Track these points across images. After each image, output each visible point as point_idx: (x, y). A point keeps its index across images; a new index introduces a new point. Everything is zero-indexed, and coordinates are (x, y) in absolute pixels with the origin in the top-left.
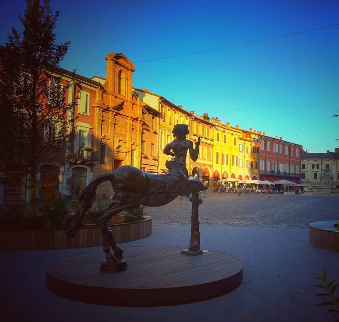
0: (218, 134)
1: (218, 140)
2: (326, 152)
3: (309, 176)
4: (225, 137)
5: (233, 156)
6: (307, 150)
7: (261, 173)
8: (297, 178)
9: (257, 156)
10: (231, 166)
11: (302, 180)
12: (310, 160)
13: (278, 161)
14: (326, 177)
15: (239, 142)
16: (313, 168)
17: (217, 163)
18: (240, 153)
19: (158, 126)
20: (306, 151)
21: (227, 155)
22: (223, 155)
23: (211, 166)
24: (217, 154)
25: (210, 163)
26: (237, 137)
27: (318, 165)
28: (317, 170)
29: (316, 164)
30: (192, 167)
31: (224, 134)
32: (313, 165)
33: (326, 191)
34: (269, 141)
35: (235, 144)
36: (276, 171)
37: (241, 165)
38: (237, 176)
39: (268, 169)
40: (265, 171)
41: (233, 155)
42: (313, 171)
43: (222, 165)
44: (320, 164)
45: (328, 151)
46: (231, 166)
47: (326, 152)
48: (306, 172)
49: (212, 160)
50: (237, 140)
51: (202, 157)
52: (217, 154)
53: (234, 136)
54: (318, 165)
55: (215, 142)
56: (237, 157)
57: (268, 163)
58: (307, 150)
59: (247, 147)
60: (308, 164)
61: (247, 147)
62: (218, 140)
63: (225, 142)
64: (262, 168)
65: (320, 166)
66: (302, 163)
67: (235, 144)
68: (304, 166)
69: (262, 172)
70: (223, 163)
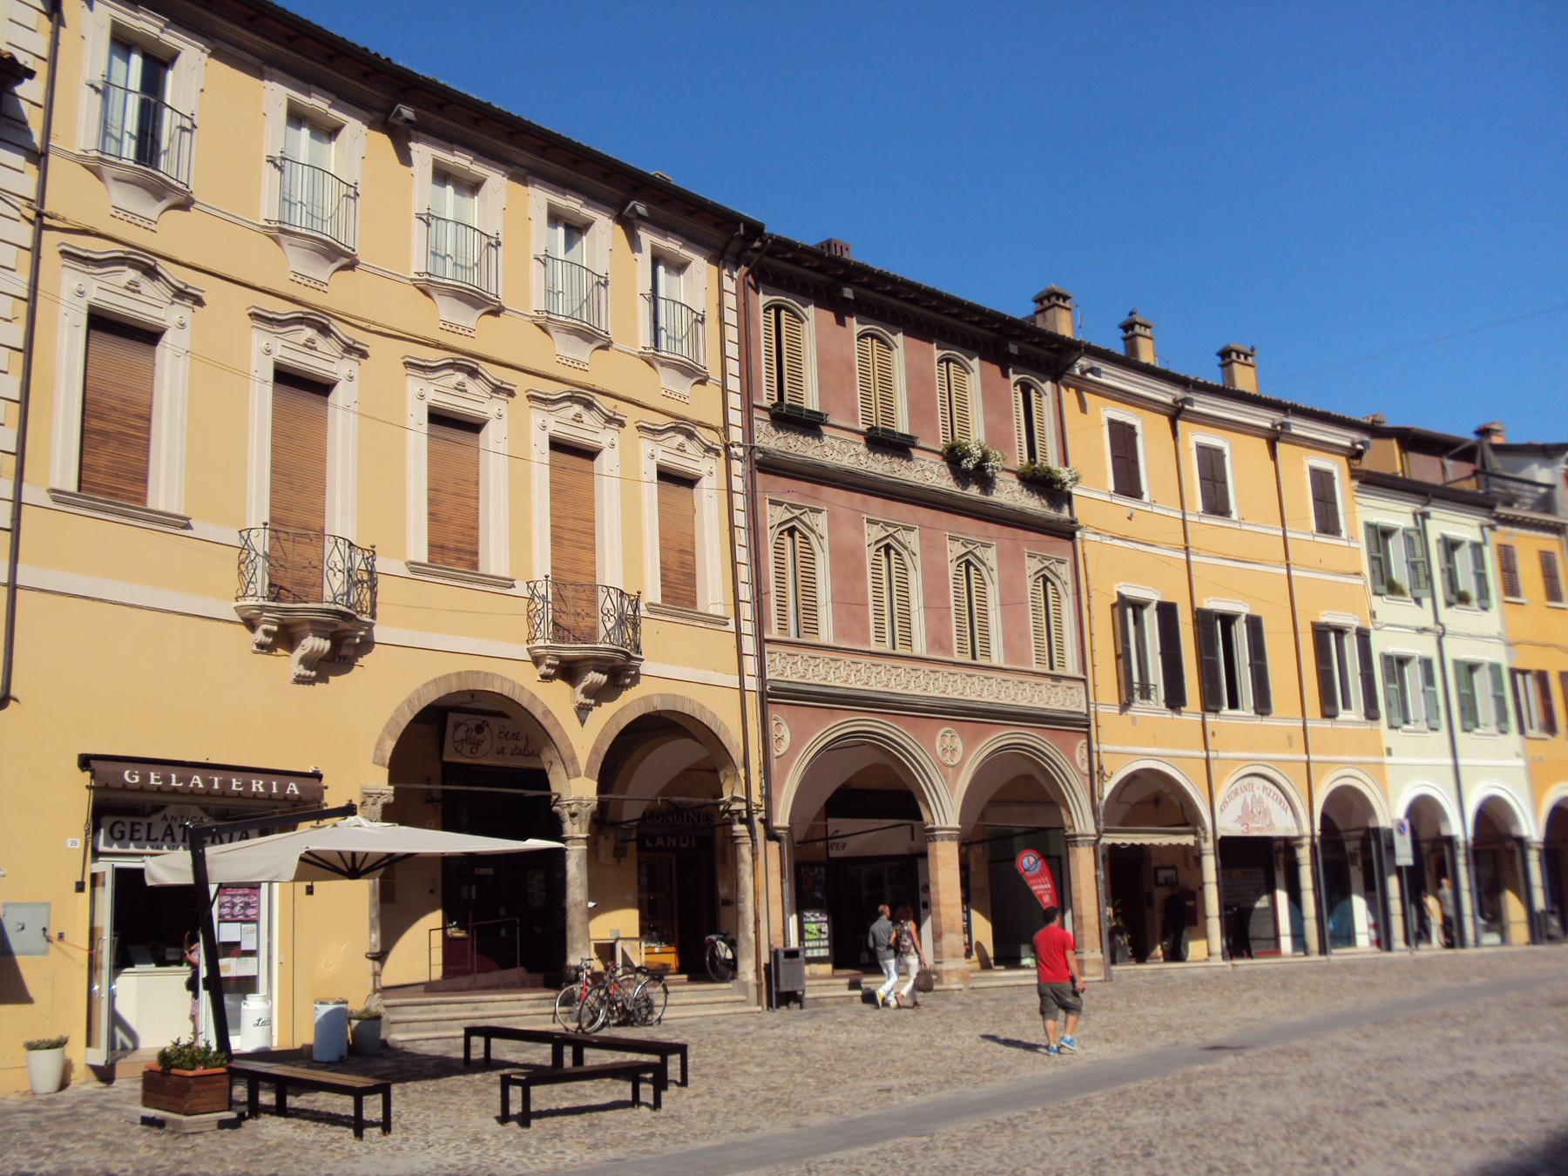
0: (1123, 437)
1: (1128, 483)
4: (1211, 462)
5: (1321, 633)
18: (1390, 610)
21: (1254, 624)
23: (1079, 725)
26: (1337, 467)
30: (794, 748)
31: (1194, 436)
35: (1328, 522)
41: (1326, 617)
43: (1210, 718)
46: (1316, 723)
49: (1072, 668)
50: (1343, 486)
51: (937, 641)
53: (1300, 464)
56: (1363, 636)
62: (1128, 483)
63: (1217, 504)
67: (1328, 522)
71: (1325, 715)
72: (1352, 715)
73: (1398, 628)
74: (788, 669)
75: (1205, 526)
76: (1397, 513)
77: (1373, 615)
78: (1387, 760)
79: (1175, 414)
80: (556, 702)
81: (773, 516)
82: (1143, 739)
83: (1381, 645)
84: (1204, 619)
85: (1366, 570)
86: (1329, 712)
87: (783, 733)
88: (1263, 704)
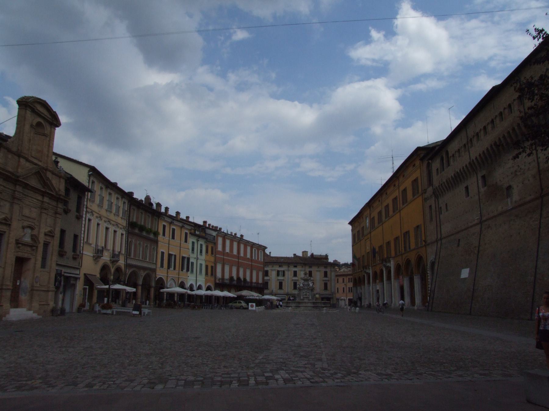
1: (164, 234)
2: (293, 256)
3: (273, 285)
4: (174, 230)
6: (270, 253)
7: (217, 282)
8: (262, 288)
9: (212, 259)
11: (266, 291)
13: (238, 266)
14: (306, 288)
15: (191, 240)
16: (278, 275)
17: (162, 266)
19: (85, 210)
20: (269, 254)
21: (175, 256)
22: (170, 255)
24: (163, 253)
25: (153, 267)
27: (284, 272)
28: (282, 278)
32: (278, 271)
33: (307, 305)
34: (228, 239)
35: (186, 241)
36: (235, 278)
38: (187, 285)
39: (227, 276)
40: (223, 278)
42: (278, 280)
45: (295, 255)
47: (293, 256)
48: (269, 280)
49: (155, 262)
52: (163, 253)
54: (284, 272)
55: (160, 237)
56: (188, 259)
57: (227, 268)
58: (270, 253)
59: (201, 245)
60: (272, 270)
61: (201, 245)
62: (164, 234)
63: (173, 238)
64: (219, 275)
65: (286, 273)
66: (266, 269)
67: (186, 241)
68: (266, 273)
69: (219, 279)
70: (169, 267)
72: (185, 270)
74: (130, 262)
75: (171, 240)
79: (171, 223)
80: (111, 265)
81: (130, 240)
82: (161, 273)
84: (170, 255)
86: (182, 270)
87: (127, 270)
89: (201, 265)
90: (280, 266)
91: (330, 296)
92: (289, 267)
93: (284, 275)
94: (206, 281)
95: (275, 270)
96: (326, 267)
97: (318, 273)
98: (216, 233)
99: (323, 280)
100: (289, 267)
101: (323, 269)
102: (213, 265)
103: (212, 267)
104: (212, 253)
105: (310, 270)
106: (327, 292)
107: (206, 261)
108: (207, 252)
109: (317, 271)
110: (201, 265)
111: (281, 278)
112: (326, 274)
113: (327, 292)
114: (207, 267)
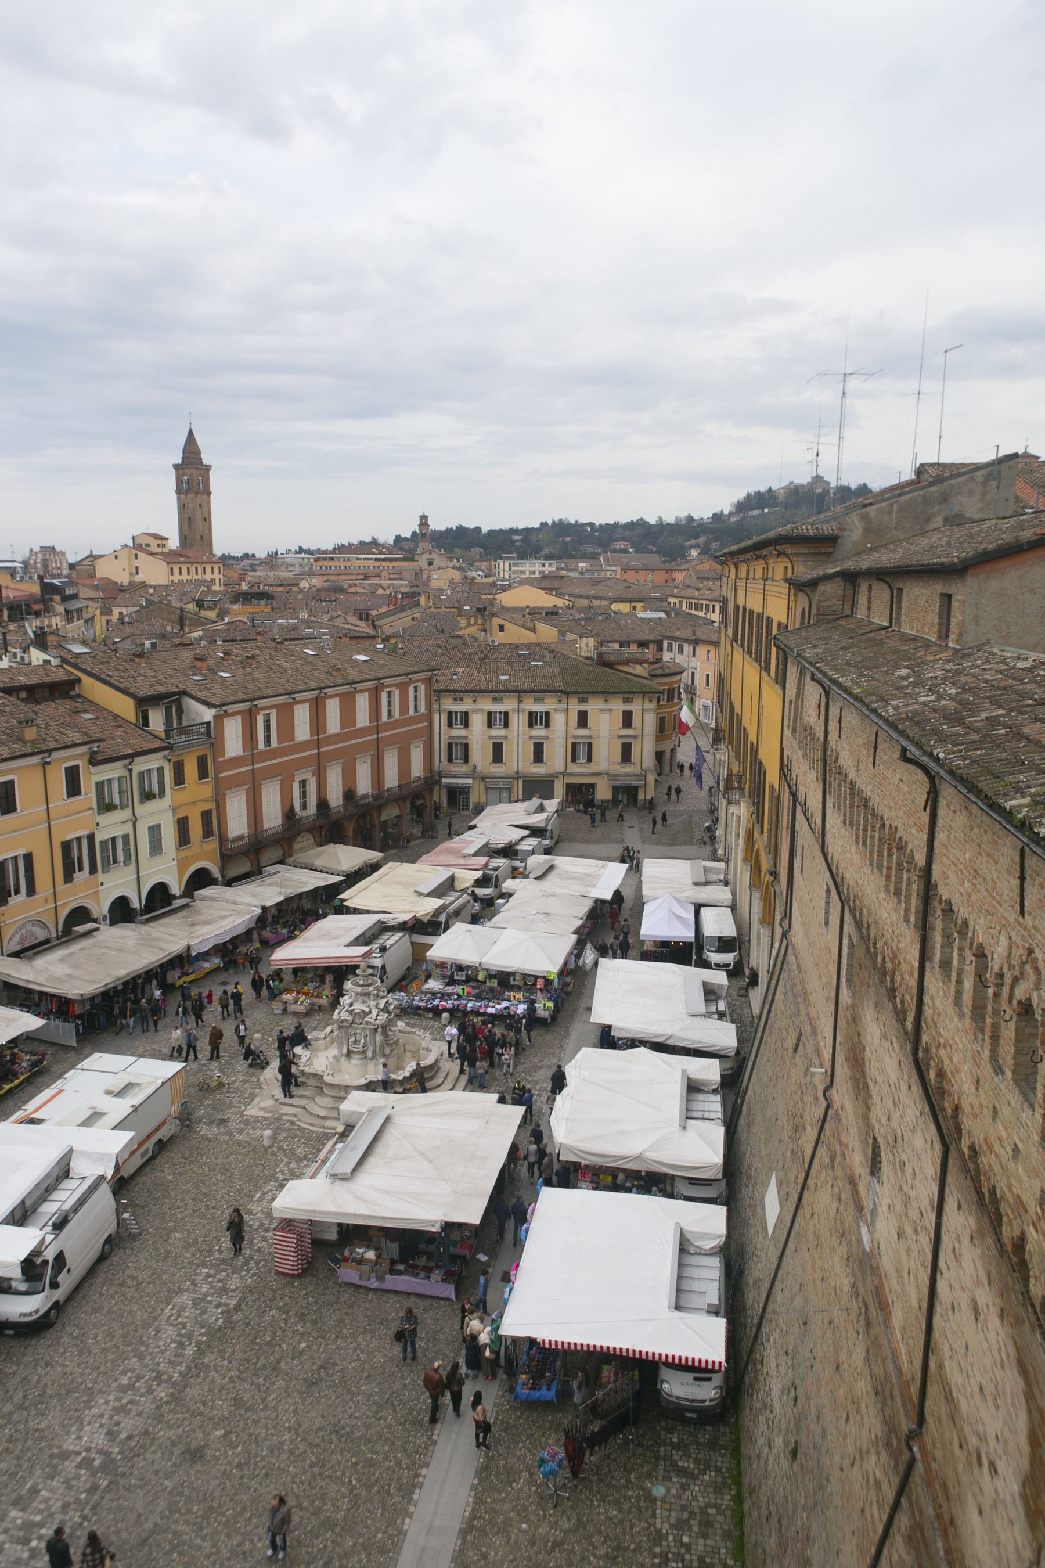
5: (66, 846)
9: (205, 790)
10: (61, 886)
12: (479, 700)
16: (490, 725)
21: (28, 858)
27: (506, 714)
28: (502, 732)
29: (500, 713)
32: (490, 714)
37: (121, 857)
42: (490, 737)
44: (513, 710)
46: (61, 886)
54: (506, 714)
56: (91, 838)
60: (474, 711)
65: (513, 718)
71: (66, 882)
73: (111, 826)
76: (113, 772)
77: (98, 824)
78: (101, 888)
83: (98, 839)
85: (95, 806)
86: (68, 877)
88: (31, 891)
89: (155, 831)
90: (495, 699)
91: (635, 783)
92: (520, 701)
93: (506, 725)
94: (182, 866)
95: (481, 711)
96: (626, 701)
97: (605, 718)
98: (213, 711)
99: (620, 737)
100: (520, 701)
101: (618, 706)
102: (211, 806)
103: (206, 815)
104: (203, 774)
105: (583, 708)
106: (628, 769)
107: (174, 810)
108: (179, 779)
109: (602, 711)
110: (155, 831)
111: (498, 732)
112: (627, 720)
113: (628, 769)
114: (182, 825)
